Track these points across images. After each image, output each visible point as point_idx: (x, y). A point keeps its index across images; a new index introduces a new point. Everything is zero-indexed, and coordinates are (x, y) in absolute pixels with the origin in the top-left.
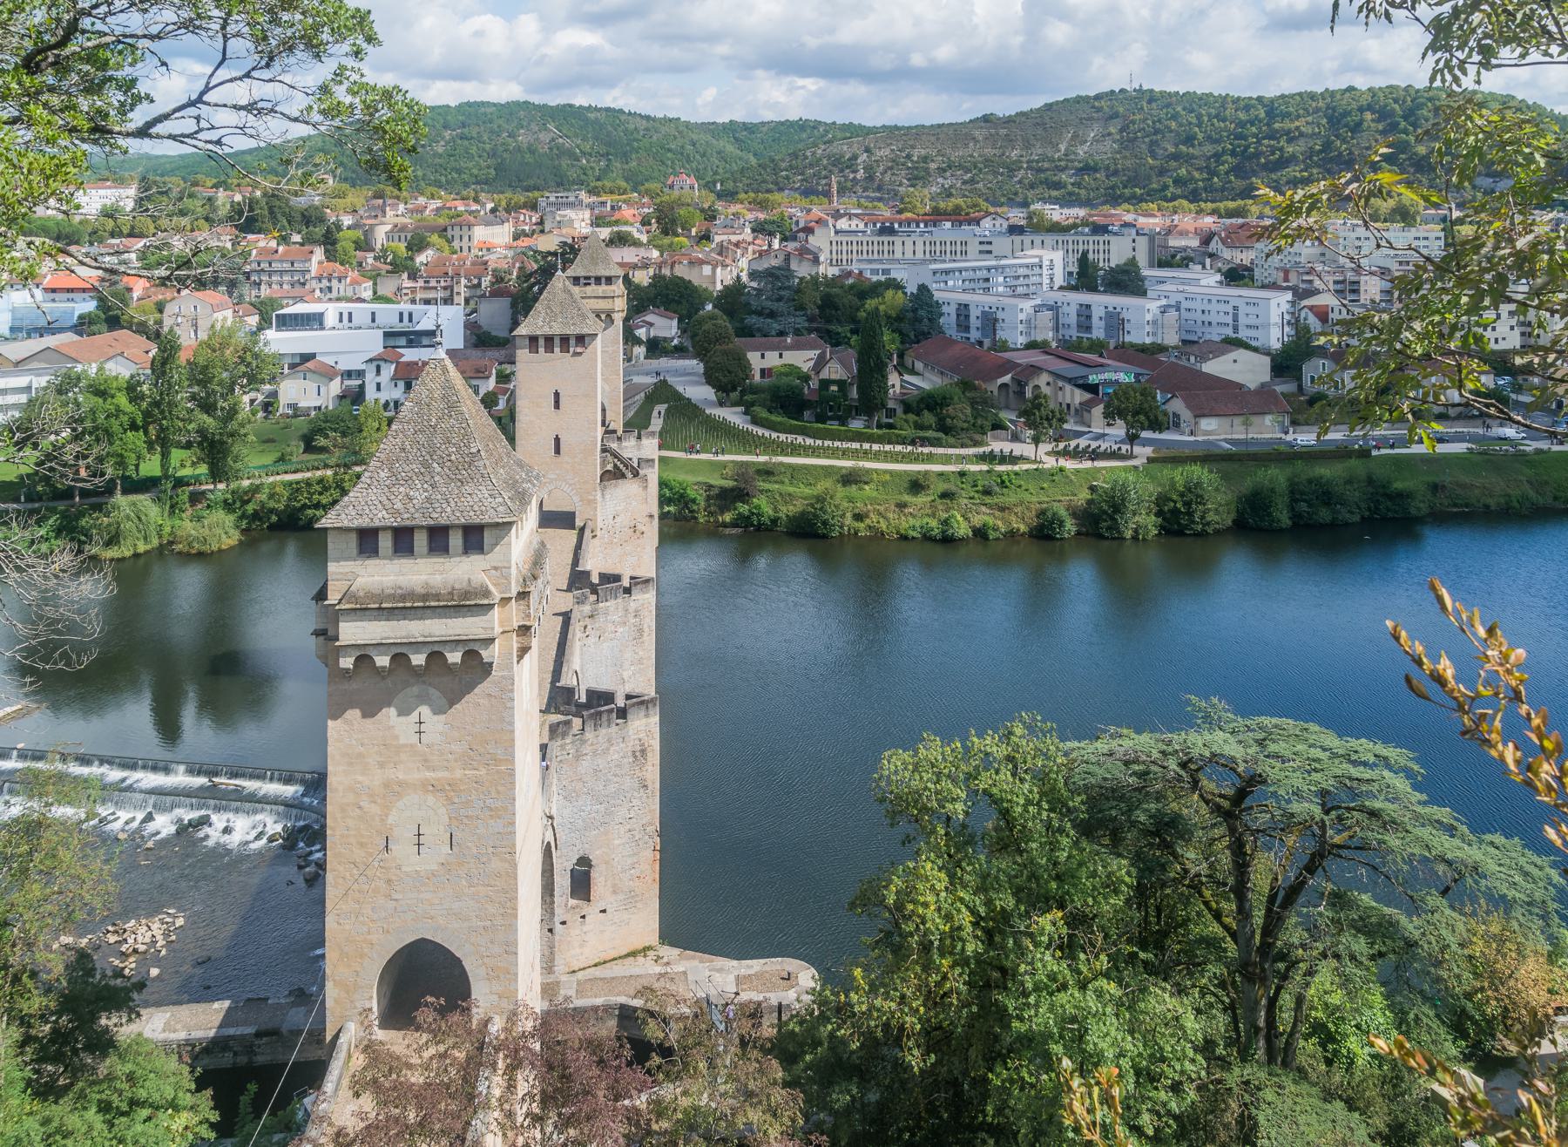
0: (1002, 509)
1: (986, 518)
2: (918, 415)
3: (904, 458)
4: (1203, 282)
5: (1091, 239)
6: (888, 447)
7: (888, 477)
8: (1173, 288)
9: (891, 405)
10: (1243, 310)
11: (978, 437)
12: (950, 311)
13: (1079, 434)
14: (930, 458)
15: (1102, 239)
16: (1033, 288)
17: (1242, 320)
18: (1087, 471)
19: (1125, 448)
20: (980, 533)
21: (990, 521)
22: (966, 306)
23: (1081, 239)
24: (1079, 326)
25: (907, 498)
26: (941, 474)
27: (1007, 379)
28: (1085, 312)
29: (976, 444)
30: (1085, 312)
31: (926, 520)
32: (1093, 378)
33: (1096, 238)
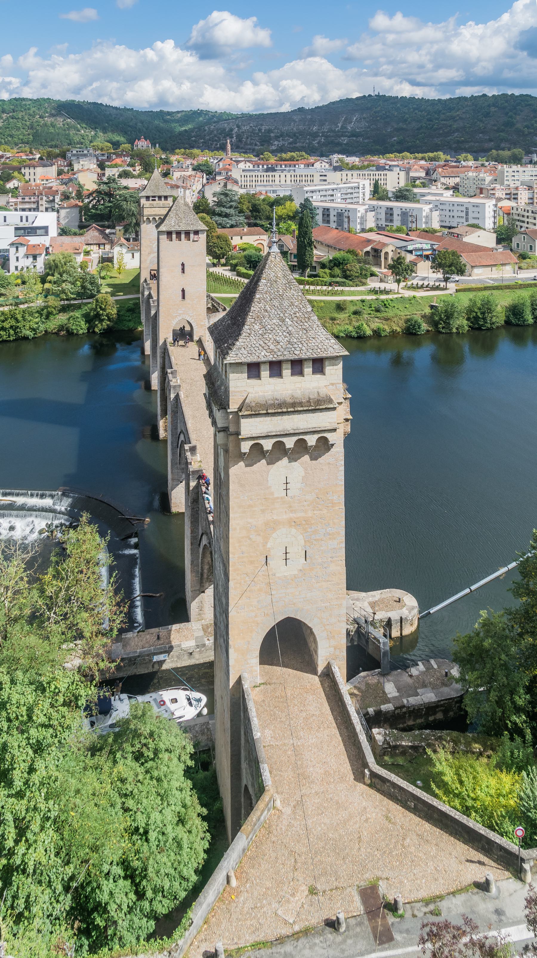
0: (387, 319)
1: (378, 324)
2: (330, 269)
3: (328, 293)
4: (444, 195)
5: (377, 173)
6: (319, 288)
7: (323, 304)
8: (434, 198)
9: (314, 264)
10: (471, 209)
11: (364, 280)
12: (320, 212)
13: (414, 278)
14: (342, 293)
15: (382, 173)
16: (355, 200)
17: (471, 215)
18: (427, 297)
19: (442, 284)
20: (377, 333)
21: (381, 326)
22: (328, 209)
23: (372, 173)
24: (386, 220)
25: (336, 315)
26: (352, 301)
27: (368, 249)
28: (390, 212)
29: (364, 284)
30: (390, 212)
31: (346, 327)
32: (410, 248)
33: (380, 172)
